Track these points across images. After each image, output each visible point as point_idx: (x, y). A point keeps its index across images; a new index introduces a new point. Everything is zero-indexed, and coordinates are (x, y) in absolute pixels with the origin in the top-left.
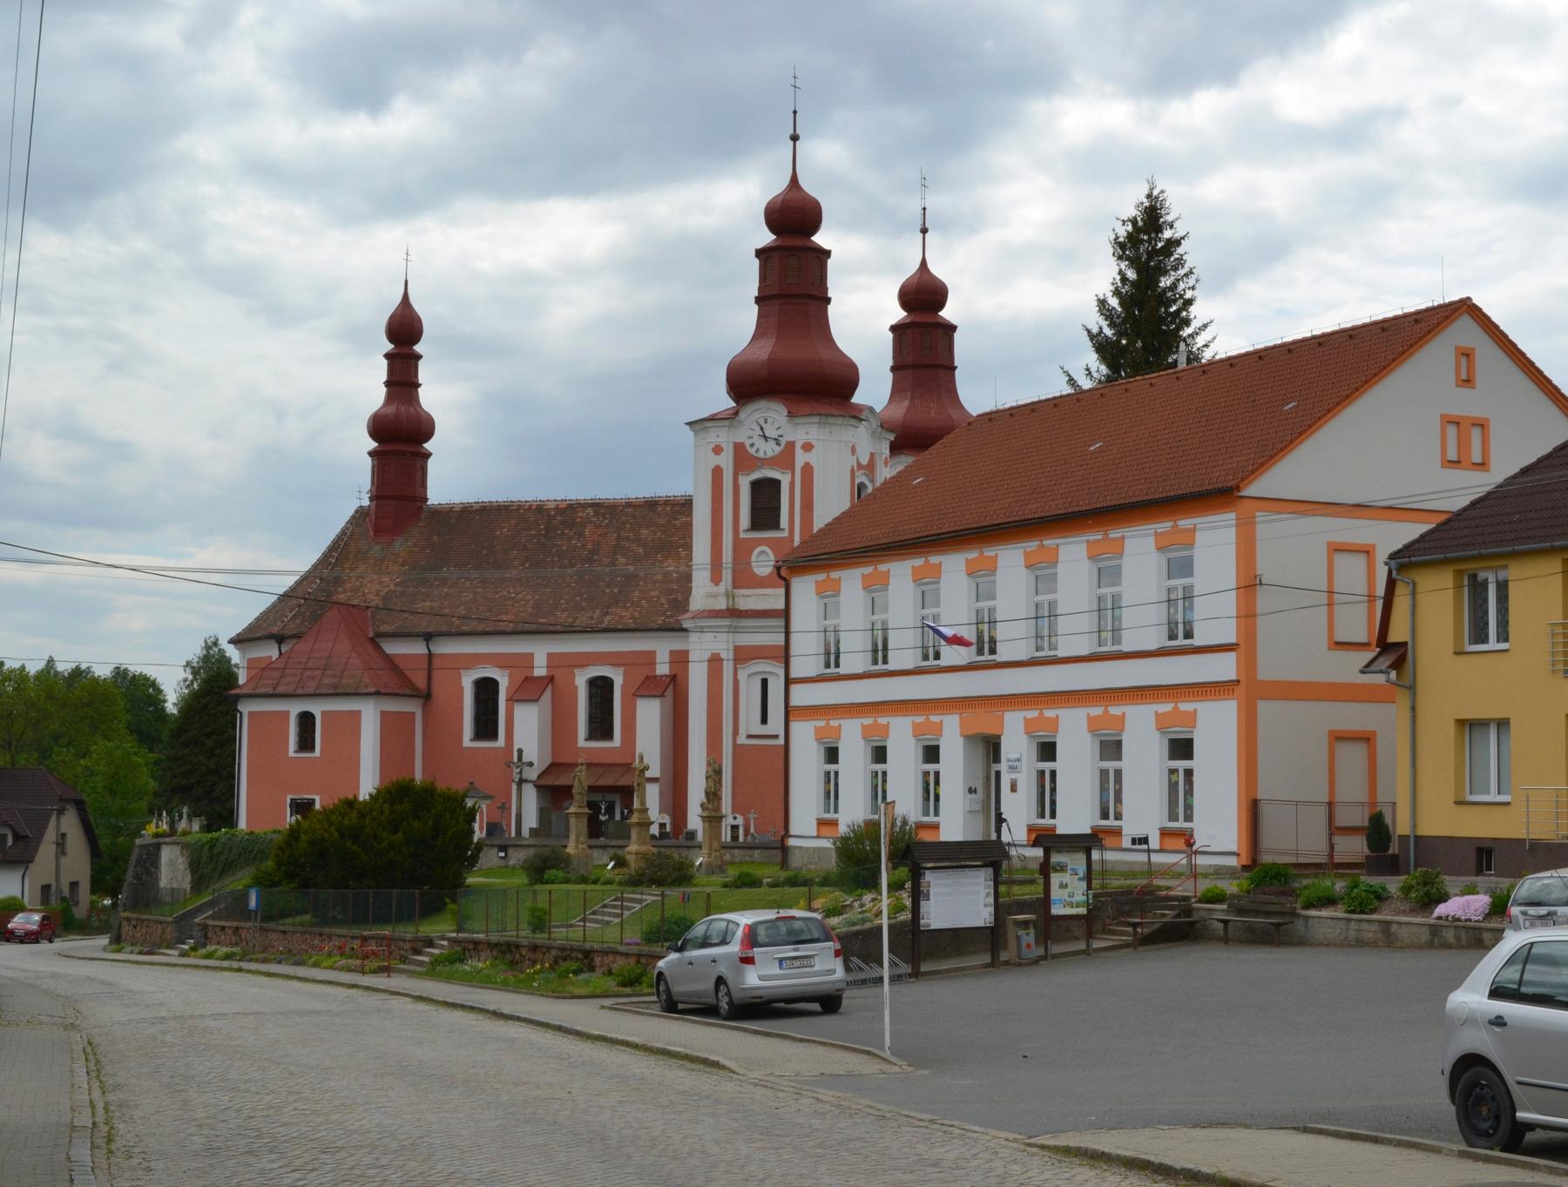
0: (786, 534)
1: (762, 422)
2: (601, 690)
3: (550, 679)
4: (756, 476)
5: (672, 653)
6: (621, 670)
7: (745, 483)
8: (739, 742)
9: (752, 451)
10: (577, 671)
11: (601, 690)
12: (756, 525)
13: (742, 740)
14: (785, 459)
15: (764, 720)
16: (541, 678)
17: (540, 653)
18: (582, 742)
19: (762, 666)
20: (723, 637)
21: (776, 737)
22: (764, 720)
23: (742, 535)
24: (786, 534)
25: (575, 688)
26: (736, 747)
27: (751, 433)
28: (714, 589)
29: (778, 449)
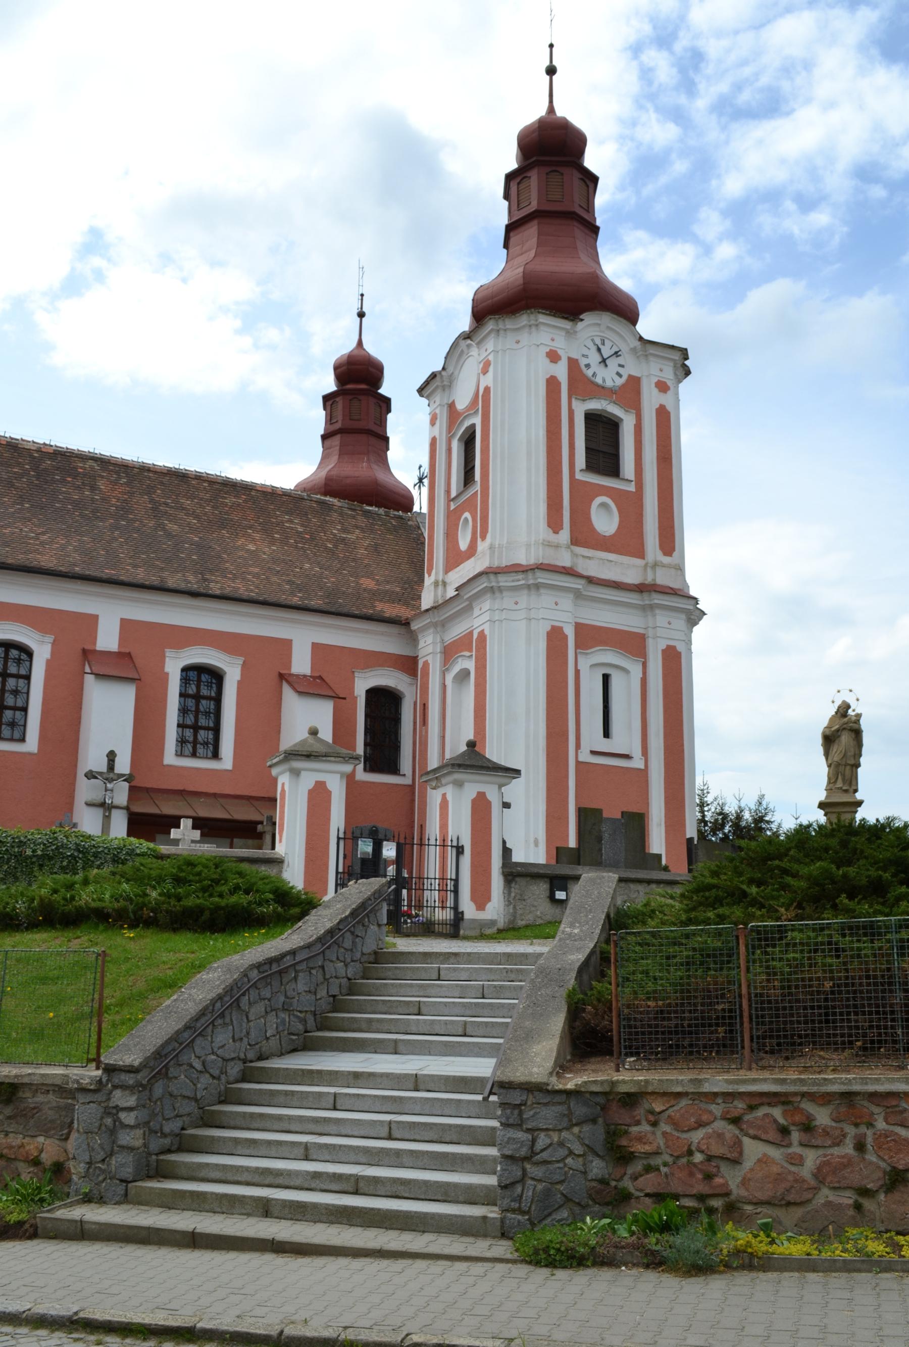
0: (632, 488)
1: (598, 342)
2: (203, 682)
3: (123, 656)
4: (595, 405)
5: (315, 646)
6: (240, 661)
7: (581, 409)
8: (581, 759)
9: (589, 373)
10: (169, 653)
11: (203, 682)
12: (591, 467)
13: (585, 757)
14: (630, 393)
15: (607, 734)
16: (107, 654)
17: (110, 618)
18: (170, 757)
19: (609, 656)
20: (567, 602)
21: (627, 757)
22: (607, 734)
23: (579, 476)
24: (632, 488)
25: (164, 678)
26: (578, 763)
27: (586, 351)
28: (552, 537)
29: (619, 382)
